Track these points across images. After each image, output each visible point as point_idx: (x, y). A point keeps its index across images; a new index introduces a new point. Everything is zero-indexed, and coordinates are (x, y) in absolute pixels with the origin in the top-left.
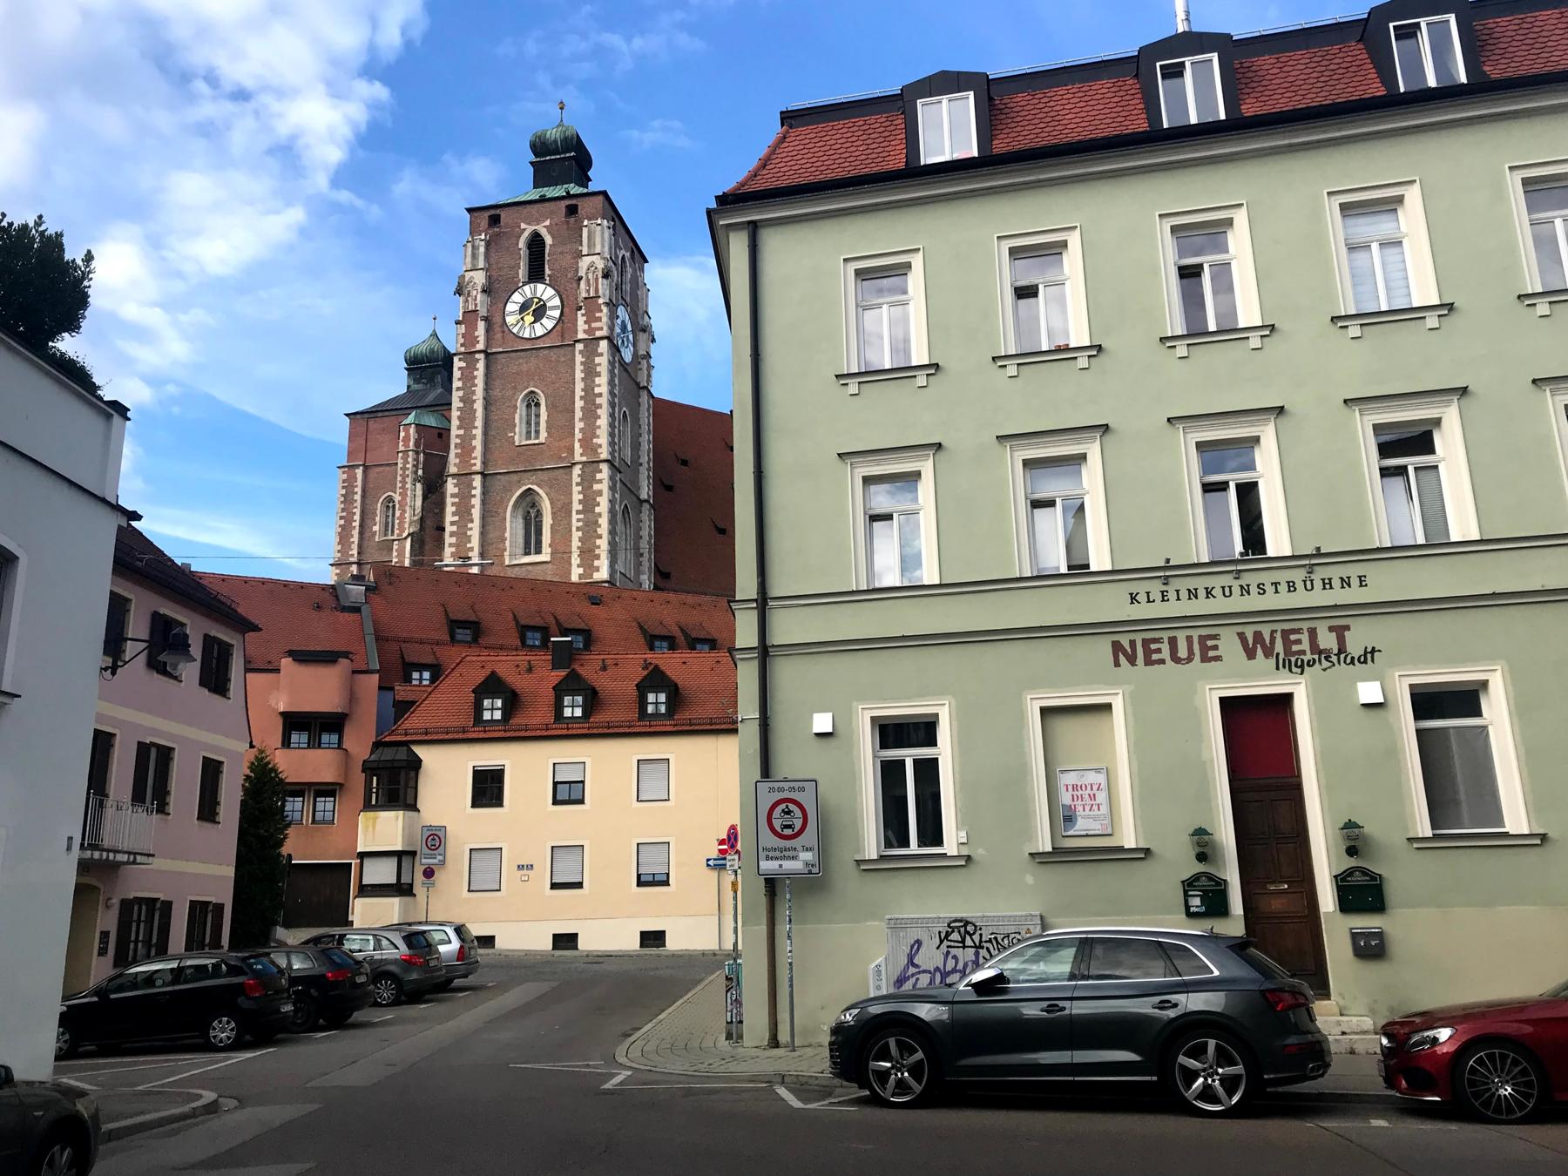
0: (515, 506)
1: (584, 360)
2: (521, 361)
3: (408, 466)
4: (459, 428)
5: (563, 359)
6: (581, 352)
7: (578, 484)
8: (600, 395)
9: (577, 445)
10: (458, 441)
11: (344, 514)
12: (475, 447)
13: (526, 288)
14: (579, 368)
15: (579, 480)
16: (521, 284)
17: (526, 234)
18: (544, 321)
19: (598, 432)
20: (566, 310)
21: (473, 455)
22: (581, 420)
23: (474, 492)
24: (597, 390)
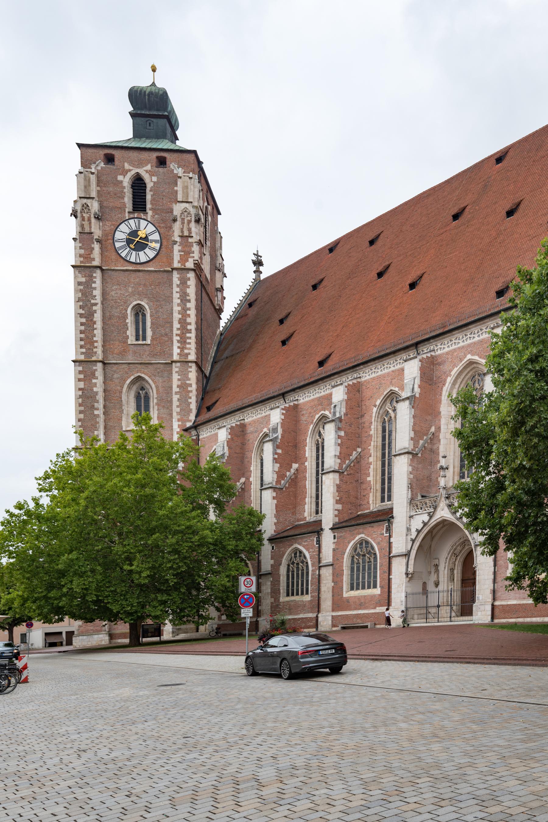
0: (129, 388)
13: (132, 222)
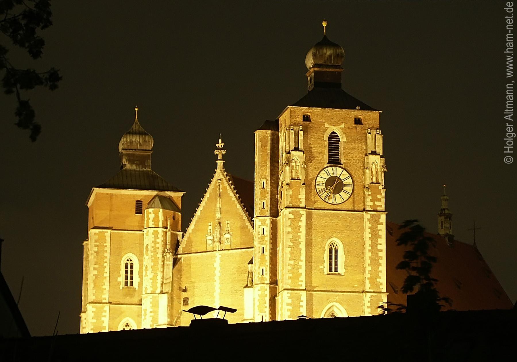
1: (370, 225)
2: (327, 218)
3: (158, 240)
4: (290, 259)
5: (354, 222)
6: (368, 220)
7: (368, 307)
8: (381, 251)
9: (367, 281)
10: (290, 268)
11: (97, 266)
12: (301, 274)
14: (368, 231)
15: (369, 304)
16: (326, 166)
17: (329, 132)
18: (342, 193)
19: (380, 275)
20: (355, 187)
21: (300, 279)
22: (369, 265)
23: (301, 304)
24: (379, 247)
